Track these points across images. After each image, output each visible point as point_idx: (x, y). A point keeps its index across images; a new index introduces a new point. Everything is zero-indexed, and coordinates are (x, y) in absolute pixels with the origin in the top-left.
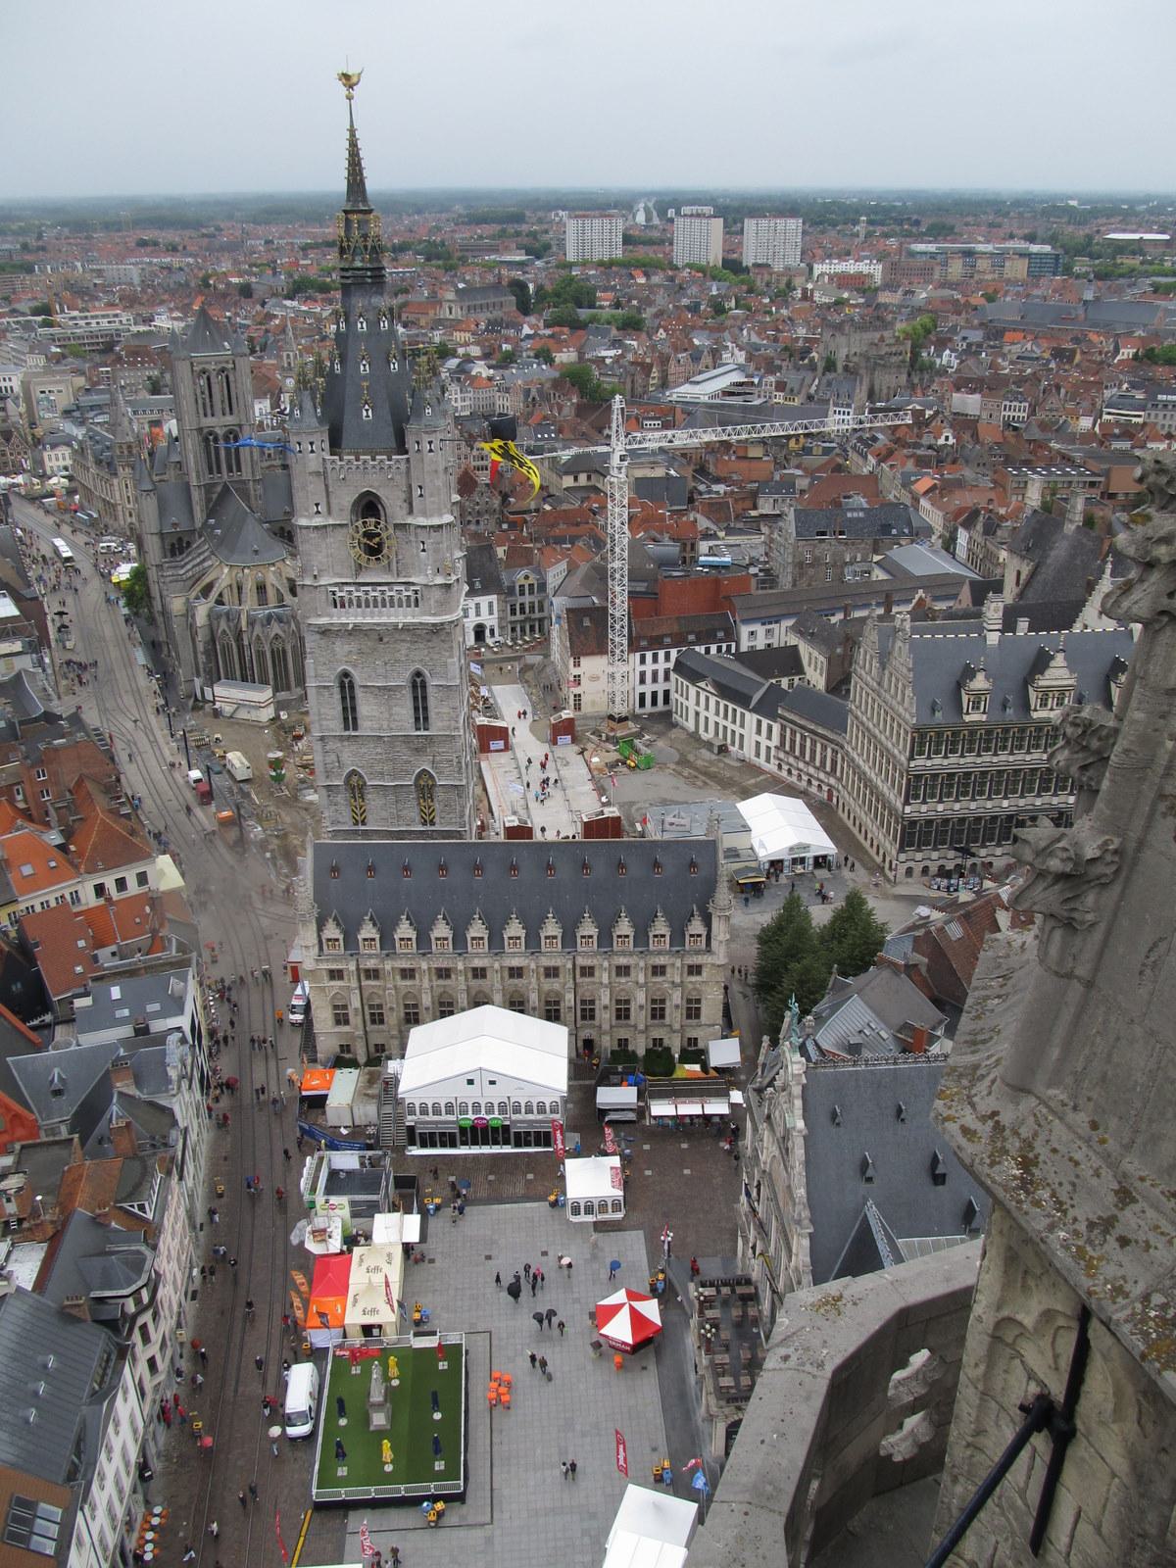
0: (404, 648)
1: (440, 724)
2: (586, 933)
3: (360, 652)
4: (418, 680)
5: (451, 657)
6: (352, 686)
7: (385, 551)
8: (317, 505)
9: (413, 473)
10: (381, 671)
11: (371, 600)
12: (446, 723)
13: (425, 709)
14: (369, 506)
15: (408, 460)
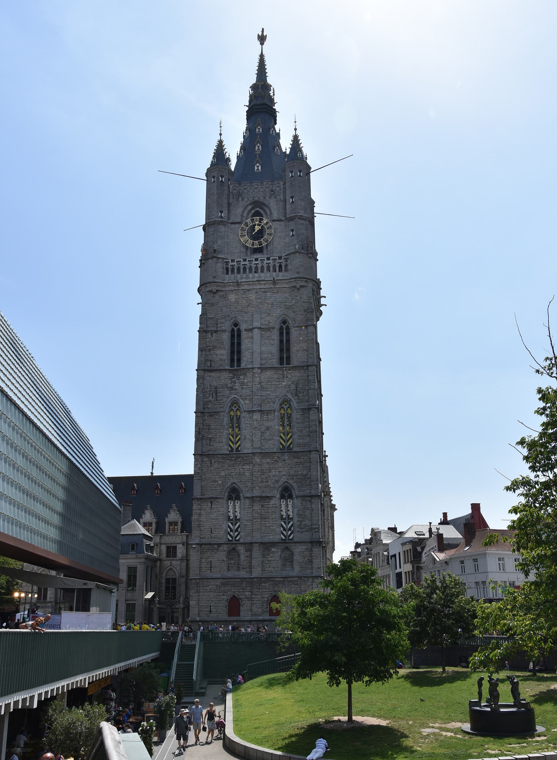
7: (266, 236)
8: (221, 212)
11: (254, 266)
15: (284, 184)
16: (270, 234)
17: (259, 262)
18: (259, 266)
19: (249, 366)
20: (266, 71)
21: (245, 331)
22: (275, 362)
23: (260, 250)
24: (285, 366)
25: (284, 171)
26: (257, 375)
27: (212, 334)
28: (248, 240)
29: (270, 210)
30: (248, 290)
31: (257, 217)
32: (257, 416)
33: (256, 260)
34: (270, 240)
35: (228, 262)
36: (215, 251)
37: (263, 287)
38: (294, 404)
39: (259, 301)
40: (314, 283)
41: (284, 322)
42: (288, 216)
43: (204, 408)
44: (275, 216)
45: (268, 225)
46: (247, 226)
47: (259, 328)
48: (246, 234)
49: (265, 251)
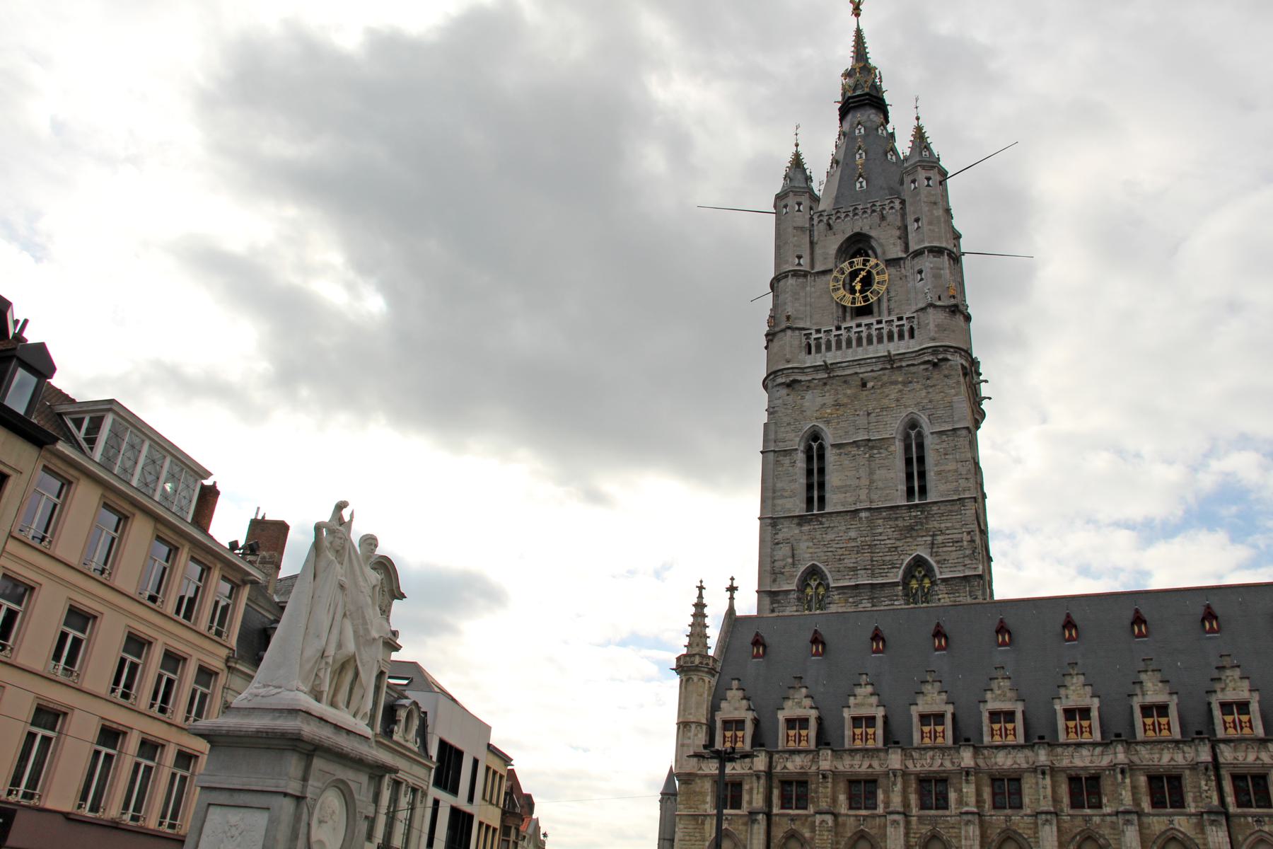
0: (893, 392)
1: (942, 487)
2: (1230, 696)
3: (837, 405)
4: (913, 433)
5: (956, 395)
6: (821, 448)
7: (875, 287)
8: (799, 257)
9: (909, 208)
10: (862, 421)
11: (854, 337)
12: (953, 486)
13: (922, 475)
14: (858, 245)
15: (903, 202)
17: (863, 328)
18: (864, 335)
20: (866, 45)
23: (866, 311)
24: (917, 502)
25: (902, 183)
28: (844, 296)
31: (860, 259)
33: (859, 325)
34: (881, 292)
35: (811, 334)
36: (788, 318)
40: (963, 353)
42: (911, 250)
45: (879, 268)
46: (843, 273)
48: (841, 286)
49: (875, 309)
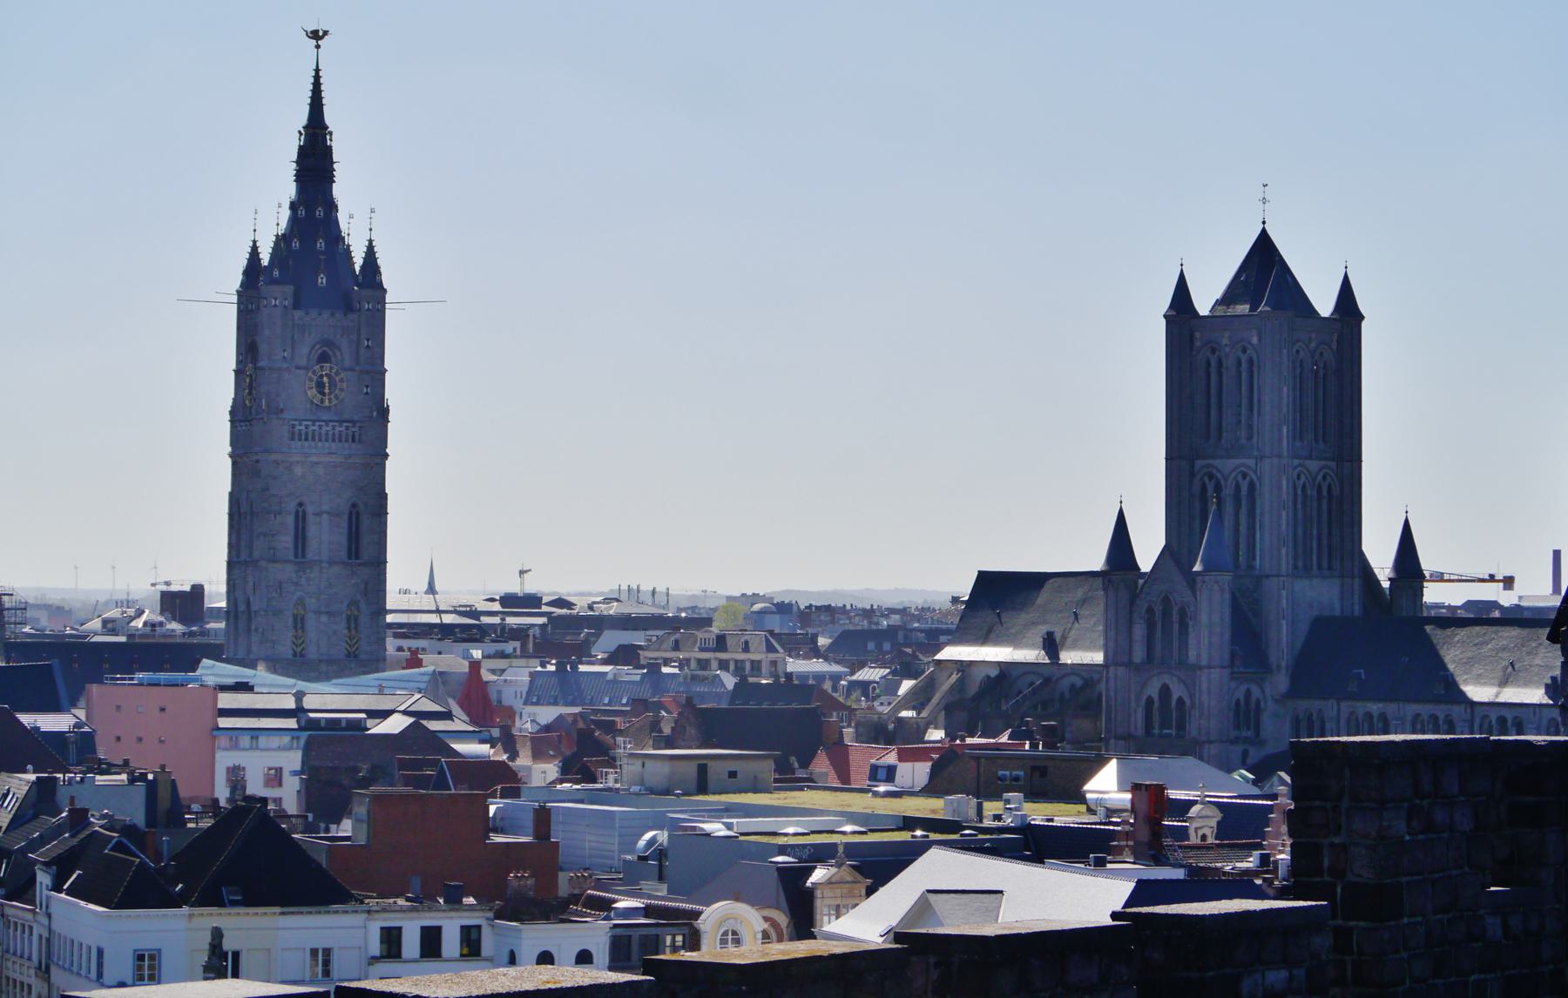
16: (342, 390)
19: (316, 558)
21: (314, 514)
22: (343, 554)
26: (325, 571)
27: (275, 516)
29: (342, 354)
30: (316, 463)
32: (324, 618)
37: (332, 460)
38: (363, 605)
39: (328, 477)
41: (354, 505)
43: (268, 605)
44: (347, 363)
47: (328, 513)
